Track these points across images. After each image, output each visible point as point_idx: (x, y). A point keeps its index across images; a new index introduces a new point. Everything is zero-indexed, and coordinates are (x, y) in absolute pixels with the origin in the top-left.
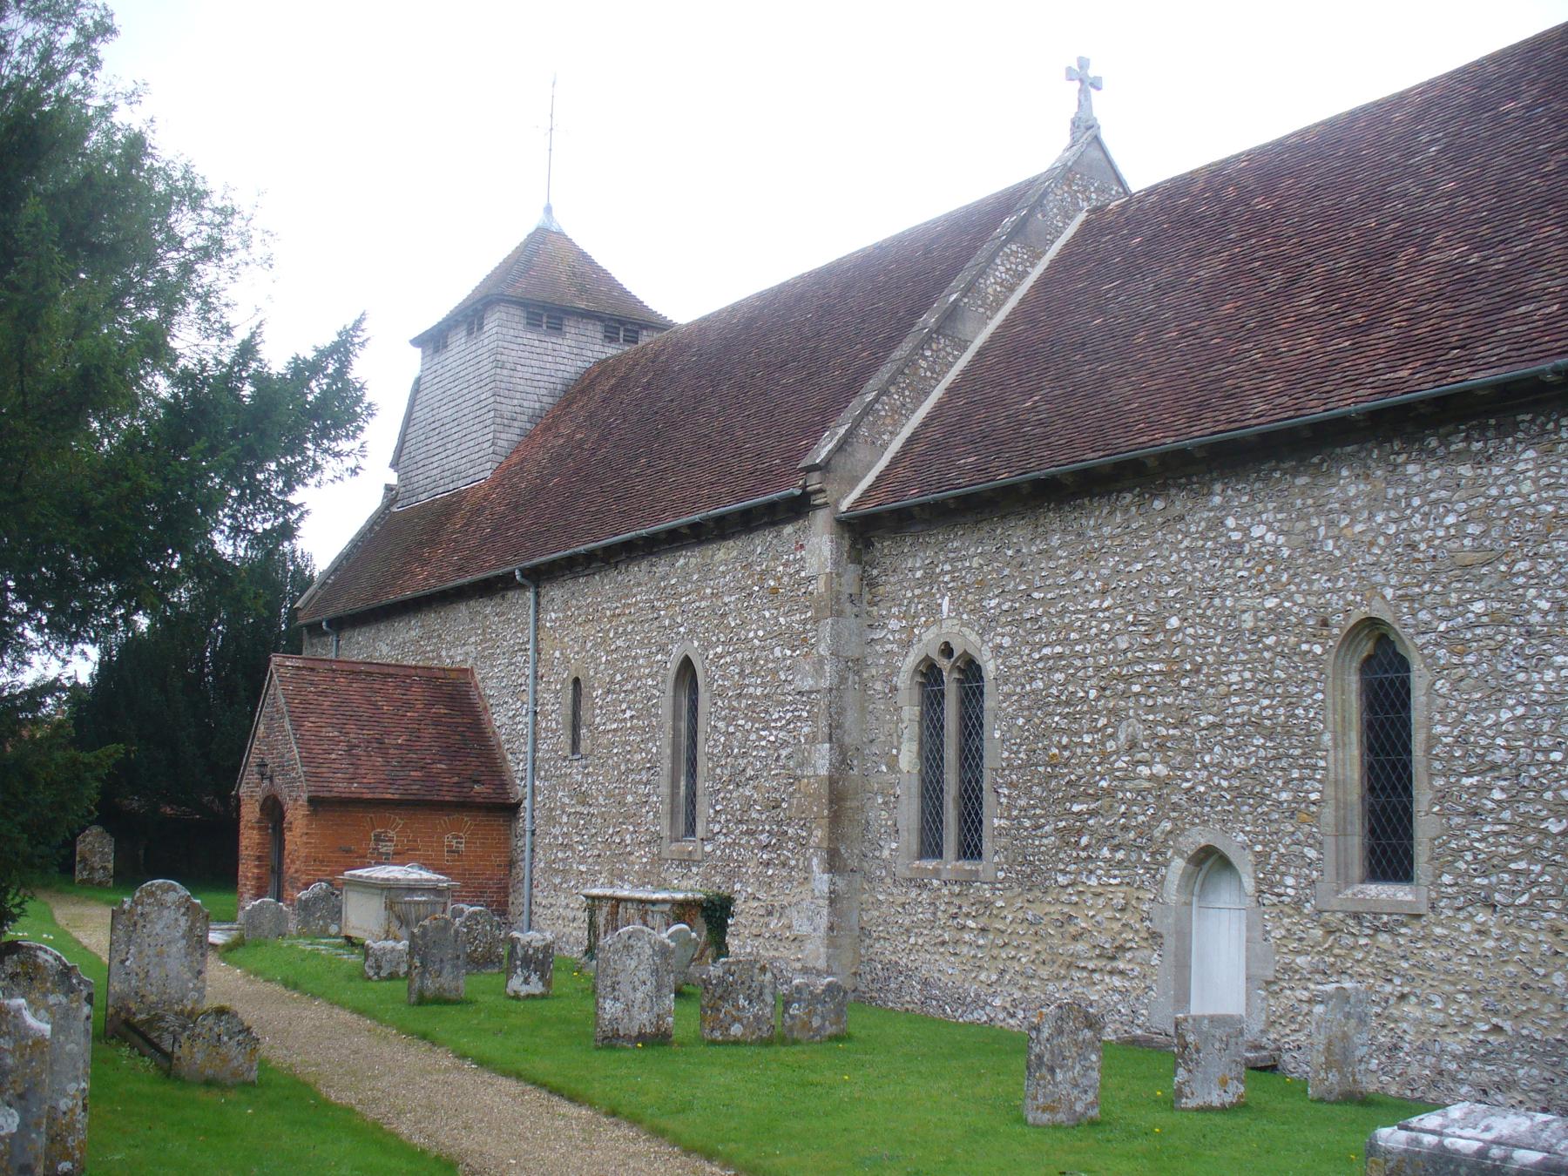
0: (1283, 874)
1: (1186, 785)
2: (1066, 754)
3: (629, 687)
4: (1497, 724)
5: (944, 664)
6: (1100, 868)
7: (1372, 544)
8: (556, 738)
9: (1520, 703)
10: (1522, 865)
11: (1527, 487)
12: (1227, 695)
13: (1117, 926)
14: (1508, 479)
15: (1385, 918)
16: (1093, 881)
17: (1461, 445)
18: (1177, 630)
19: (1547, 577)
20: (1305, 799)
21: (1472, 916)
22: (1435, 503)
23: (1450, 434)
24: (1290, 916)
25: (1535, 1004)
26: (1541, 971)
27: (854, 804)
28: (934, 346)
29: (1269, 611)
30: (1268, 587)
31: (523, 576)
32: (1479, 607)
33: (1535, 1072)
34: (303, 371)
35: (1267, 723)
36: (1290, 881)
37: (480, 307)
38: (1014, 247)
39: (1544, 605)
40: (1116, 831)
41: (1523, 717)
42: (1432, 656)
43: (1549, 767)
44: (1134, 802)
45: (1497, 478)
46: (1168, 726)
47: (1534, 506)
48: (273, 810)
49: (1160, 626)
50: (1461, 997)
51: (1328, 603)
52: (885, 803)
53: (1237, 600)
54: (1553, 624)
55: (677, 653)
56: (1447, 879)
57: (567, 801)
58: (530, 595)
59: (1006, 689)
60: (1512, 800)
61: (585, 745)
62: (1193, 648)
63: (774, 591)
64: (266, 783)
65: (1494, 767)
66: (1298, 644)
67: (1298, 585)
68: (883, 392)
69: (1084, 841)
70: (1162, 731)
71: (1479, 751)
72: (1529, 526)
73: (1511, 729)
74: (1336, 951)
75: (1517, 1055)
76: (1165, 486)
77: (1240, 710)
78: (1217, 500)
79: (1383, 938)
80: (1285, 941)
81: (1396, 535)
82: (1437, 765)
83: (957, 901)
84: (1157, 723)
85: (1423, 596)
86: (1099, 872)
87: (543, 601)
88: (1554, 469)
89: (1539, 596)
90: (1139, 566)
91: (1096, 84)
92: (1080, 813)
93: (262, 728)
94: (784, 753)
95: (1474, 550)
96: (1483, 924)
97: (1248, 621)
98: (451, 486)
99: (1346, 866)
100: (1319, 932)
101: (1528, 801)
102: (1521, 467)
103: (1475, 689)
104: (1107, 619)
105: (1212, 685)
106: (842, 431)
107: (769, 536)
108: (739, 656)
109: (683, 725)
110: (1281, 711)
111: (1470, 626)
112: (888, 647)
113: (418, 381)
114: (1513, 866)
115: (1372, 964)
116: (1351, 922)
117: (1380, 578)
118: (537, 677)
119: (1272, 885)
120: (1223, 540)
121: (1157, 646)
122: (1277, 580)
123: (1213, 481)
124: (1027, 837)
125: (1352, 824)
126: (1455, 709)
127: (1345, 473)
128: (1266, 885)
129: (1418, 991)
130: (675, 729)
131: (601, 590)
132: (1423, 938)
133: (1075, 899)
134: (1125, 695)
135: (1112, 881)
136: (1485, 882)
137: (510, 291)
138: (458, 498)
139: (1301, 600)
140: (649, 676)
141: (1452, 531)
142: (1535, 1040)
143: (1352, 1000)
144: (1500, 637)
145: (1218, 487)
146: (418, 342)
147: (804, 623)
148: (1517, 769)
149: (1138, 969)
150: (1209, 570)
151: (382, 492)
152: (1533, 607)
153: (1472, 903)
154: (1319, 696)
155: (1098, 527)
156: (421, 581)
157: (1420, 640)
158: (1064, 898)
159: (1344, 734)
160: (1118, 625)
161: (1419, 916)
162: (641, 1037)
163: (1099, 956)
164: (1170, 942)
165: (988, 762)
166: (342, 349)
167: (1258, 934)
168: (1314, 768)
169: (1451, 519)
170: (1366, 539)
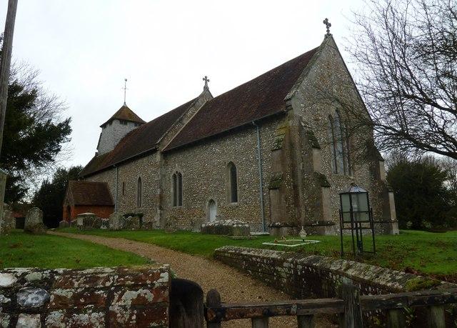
34: (61, 125)
48: (69, 208)
91: (208, 81)
131: (127, 167)
138: (108, 154)
162: (117, 230)
166: (67, 122)
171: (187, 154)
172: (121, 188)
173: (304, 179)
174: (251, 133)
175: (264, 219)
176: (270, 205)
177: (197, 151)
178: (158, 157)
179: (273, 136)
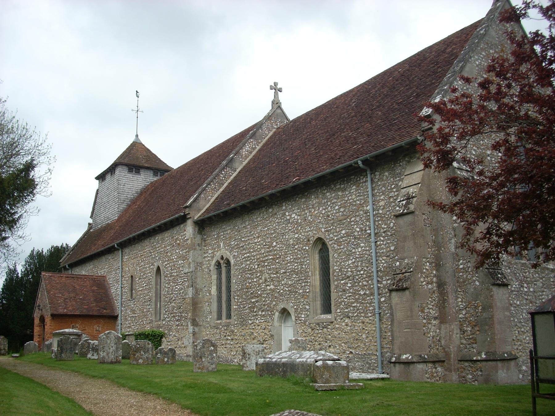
0: (301, 314)
1: (278, 291)
2: (250, 285)
3: (144, 277)
4: (348, 265)
5: (222, 262)
6: (259, 317)
7: (319, 216)
8: (127, 296)
9: (353, 258)
10: (355, 304)
11: (354, 196)
12: (287, 264)
13: (263, 334)
14: (350, 195)
15: (325, 324)
16: (258, 322)
17: (339, 186)
18: (275, 246)
19: (359, 221)
20: (306, 292)
21: (345, 321)
22: (333, 203)
23: (336, 183)
24: (303, 326)
25: (359, 344)
26: (360, 334)
27: (200, 305)
28: (225, 170)
29: (296, 238)
30: (296, 231)
31: (117, 246)
32: (343, 232)
33: (360, 363)
35: (296, 270)
36: (303, 316)
37: (114, 166)
38: (252, 140)
39: (358, 230)
40: (262, 306)
41: (354, 262)
42: (333, 247)
43: (360, 276)
44: (266, 297)
45: (347, 195)
46: (274, 274)
47: (355, 202)
48: (42, 319)
49: (270, 246)
50: (343, 344)
51: (309, 234)
52: (208, 305)
53: (289, 236)
54: (360, 235)
55: (156, 264)
56: (338, 311)
57: (130, 313)
58: (120, 252)
59: (236, 268)
60: (352, 286)
61: (134, 295)
62: (279, 251)
63: (179, 244)
64: (40, 312)
65: (348, 277)
66: (303, 247)
67: (303, 230)
68: (209, 184)
69: (255, 310)
70: (272, 276)
71: (345, 273)
72: (354, 208)
73: (352, 266)
74: (314, 335)
75: (356, 359)
76: (272, 205)
77: (290, 267)
78: (284, 208)
79: (325, 329)
80: (303, 334)
81: (325, 213)
82: (335, 278)
83: (226, 332)
84: (271, 273)
85: (331, 230)
86: (259, 319)
87: (124, 253)
88: (359, 191)
89: (357, 227)
90: (266, 229)
91: (280, 90)
92: (254, 302)
93: (40, 295)
94: (181, 292)
95: (342, 216)
96: (347, 323)
97: (291, 242)
98: (107, 223)
99: (316, 310)
100: (310, 330)
101: (356, 286)
102: (352, 191)
103: (343, 255)
104: (259, 245)
105: (283, 261)
106: (195, 196)
107: (177, 228)
108: (171, 264)
109: (158, 287)
110: (299, 267)
111: (342, 238)
112: (209, 258)
113: (98, 190)
114: (353, 305)
115: (322, 338)
116: (317, 326)
117: (321, 226)
118: (122, 276)
119: (299, 317)
120: (285, 219)
121: (271, 251)
122: (298, 229)
123: (283, 202)
124: (242, 311)
125: (317, 298)
126: (339, 261)
127: (313, 197)
128: (298, 318)
129: (333, 344)
130: (156, 288)
132: (334, 328)
133: (253, 327)
134: (263, 266)
135: (262, 321)
136: (347, 310)
137: (123, 161)
139: (303, 234)
140: (149, 273)
141: (337, 211)
142: (359, 355)
143: (301, 343)
144: (348, 240)
145: (284, 204)
146: (97, 178)
147: (186, 252)
148: (353, 277)
149: (268, 346)
150: (282, 228)
151: (88, 225)
152: (356, 230)
153: (344, 317)
154: (308, 261)
155: (257, 218)
156: (94, 250)
157: (330, 243)
158: (251, 327)
159: (314, 272)
160: (262, 246)
161: (332, 322)
162: (112, 363)
163: (259, 344)
164: (275, 337)
165: (232, 290)
167: (296, 332)
168: (307, 282)
169: (337, 208)
170: (318, 215)
171: (239, 223)
172: (127, 285)
173: (458, 270)
174: (357, 183)
175: (382, 348)
176: (392, 321)
177: (258, 218)
178: (189, 229)
179: (399, 189)
